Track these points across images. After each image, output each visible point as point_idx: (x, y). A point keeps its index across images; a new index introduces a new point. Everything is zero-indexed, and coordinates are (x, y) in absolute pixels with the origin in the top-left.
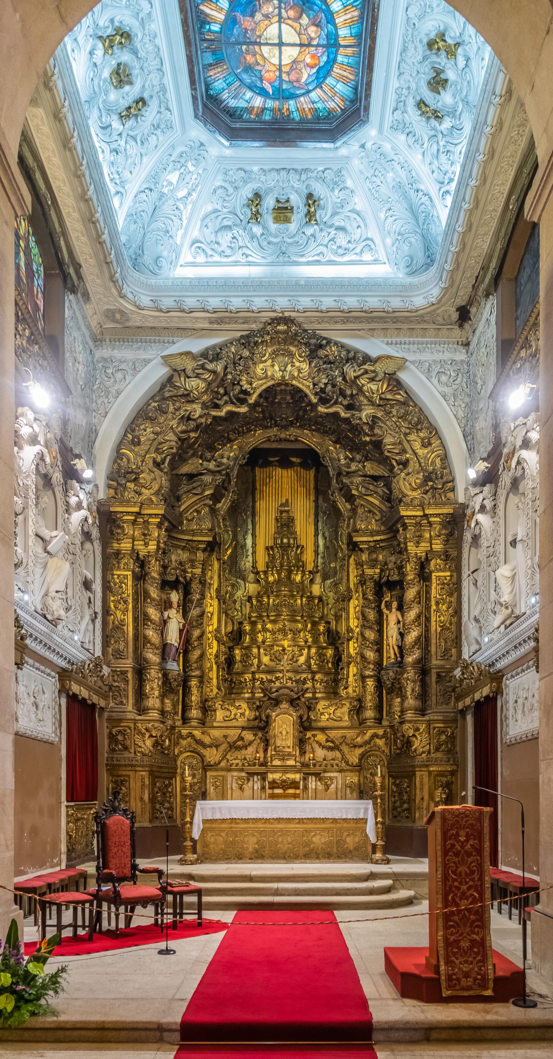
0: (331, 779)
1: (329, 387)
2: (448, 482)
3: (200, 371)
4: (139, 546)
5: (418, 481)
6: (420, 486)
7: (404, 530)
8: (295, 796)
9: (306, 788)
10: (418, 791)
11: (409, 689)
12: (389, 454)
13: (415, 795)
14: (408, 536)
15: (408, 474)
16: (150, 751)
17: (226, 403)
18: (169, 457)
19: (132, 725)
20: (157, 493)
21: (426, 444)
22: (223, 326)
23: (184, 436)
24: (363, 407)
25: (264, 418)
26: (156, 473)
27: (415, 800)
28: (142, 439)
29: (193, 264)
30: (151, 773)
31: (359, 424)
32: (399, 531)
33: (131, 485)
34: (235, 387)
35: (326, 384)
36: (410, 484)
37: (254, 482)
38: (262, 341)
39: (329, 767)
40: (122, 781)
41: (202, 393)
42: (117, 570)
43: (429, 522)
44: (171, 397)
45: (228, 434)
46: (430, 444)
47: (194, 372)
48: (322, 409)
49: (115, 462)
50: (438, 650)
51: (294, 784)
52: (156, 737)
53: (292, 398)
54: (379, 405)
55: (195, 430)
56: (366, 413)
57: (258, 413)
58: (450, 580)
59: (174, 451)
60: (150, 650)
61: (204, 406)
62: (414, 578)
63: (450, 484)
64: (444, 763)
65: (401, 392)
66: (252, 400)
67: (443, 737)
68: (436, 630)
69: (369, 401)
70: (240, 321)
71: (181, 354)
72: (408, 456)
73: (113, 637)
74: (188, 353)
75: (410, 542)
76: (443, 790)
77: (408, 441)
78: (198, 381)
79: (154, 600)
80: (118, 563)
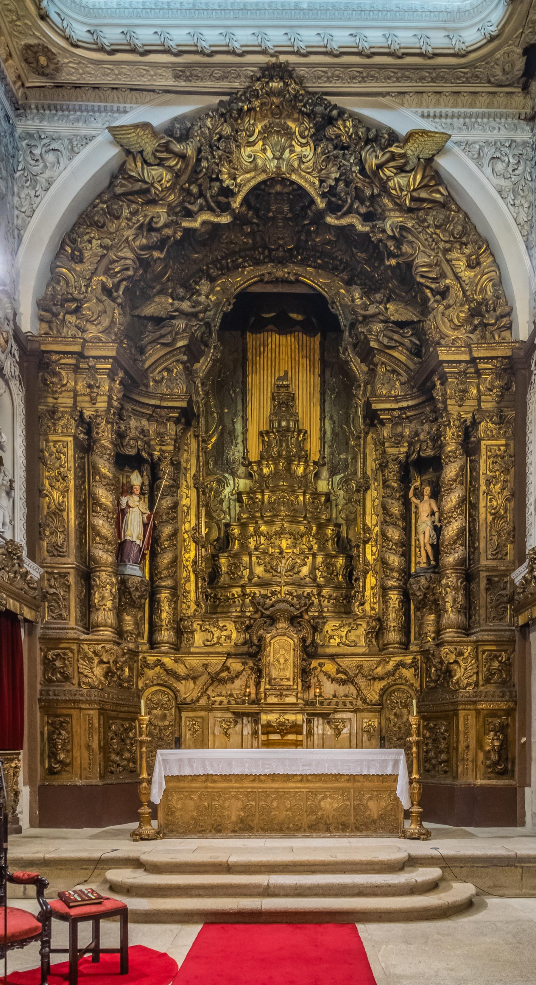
0: (343, 721)
1: (342, 185)
2: (503, 316)
3: (163, 155)
4: (84, 403)
5: (462, 315)
7: (442, 384)
8: (297, 744)
9: (310, 733)
10: (461, 736)
11: (449, 599)
12: (422, 280)
13: (458, 742)
14: (448, 391)
15: (447, 307)
16: (101, 682)
17: (201, 209)
18: (124, 283)
19: (75, 647)
22: (193, 84)
23: (145, 254)
24: (387, 213)
25: (254, 248)
26: (106, 303)
27: (457, 749)
28: (87, 254)
30: (102, 712)
31: (380, 240)
32: (435, 385)
34: (213, 184)
35: (337, 180)
36: (451, 321)
37: (244, 351)
38: (249, 110)
39: (341, 706)
40: (61, 723)
41: (168, 189)
42: (53, 434)
43: (478, 373)
44: (124, 194)
45: (208, 268)
46: (479, 264)
47: (156, 157)
48: (330, 220)
49: (48, 285)
50: (489, 546)
51: (295, 728)
52: (108, 663)
53: (291, 211)
54: (410, 210)
55: (160, 245)
57: (247, 235)
58: (505, 451)
59: (130, 273)
60: (100, 546)
61: (171, 209)
62: (457, 449)
63: (505, 321)
64: (497, 699)
65: (441, 189)
66: (236, 203)
67: (496, 664)
68: (486, 518)
69: (396, 203)
70: (218, 73)
71: (136, 126)
72: (447, 281)
73: (48, 526)
74: (146, 126)
75: (451, 398)
76: (495, 735)
77: (448, 261)
78: (161, 170)
79: (104, 476)
80: (54, 424)
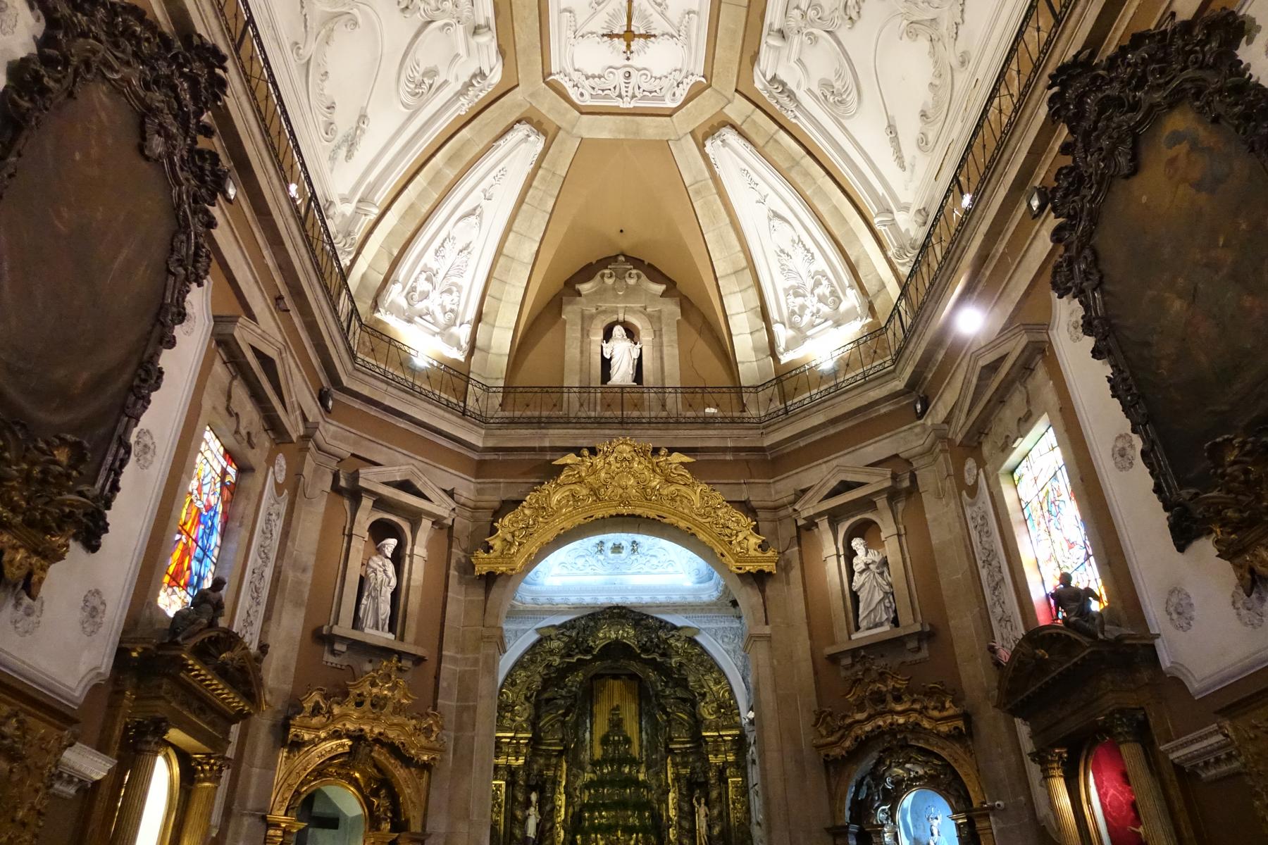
1: (648, 643)
4: (512, 760)
6: (715, 712)
20: (526, 721)
21: (717, 682)
29: (560, 575)
33: (509, 715)
56: (674, 661)
61: (562, 657)
79: (519, 802)
